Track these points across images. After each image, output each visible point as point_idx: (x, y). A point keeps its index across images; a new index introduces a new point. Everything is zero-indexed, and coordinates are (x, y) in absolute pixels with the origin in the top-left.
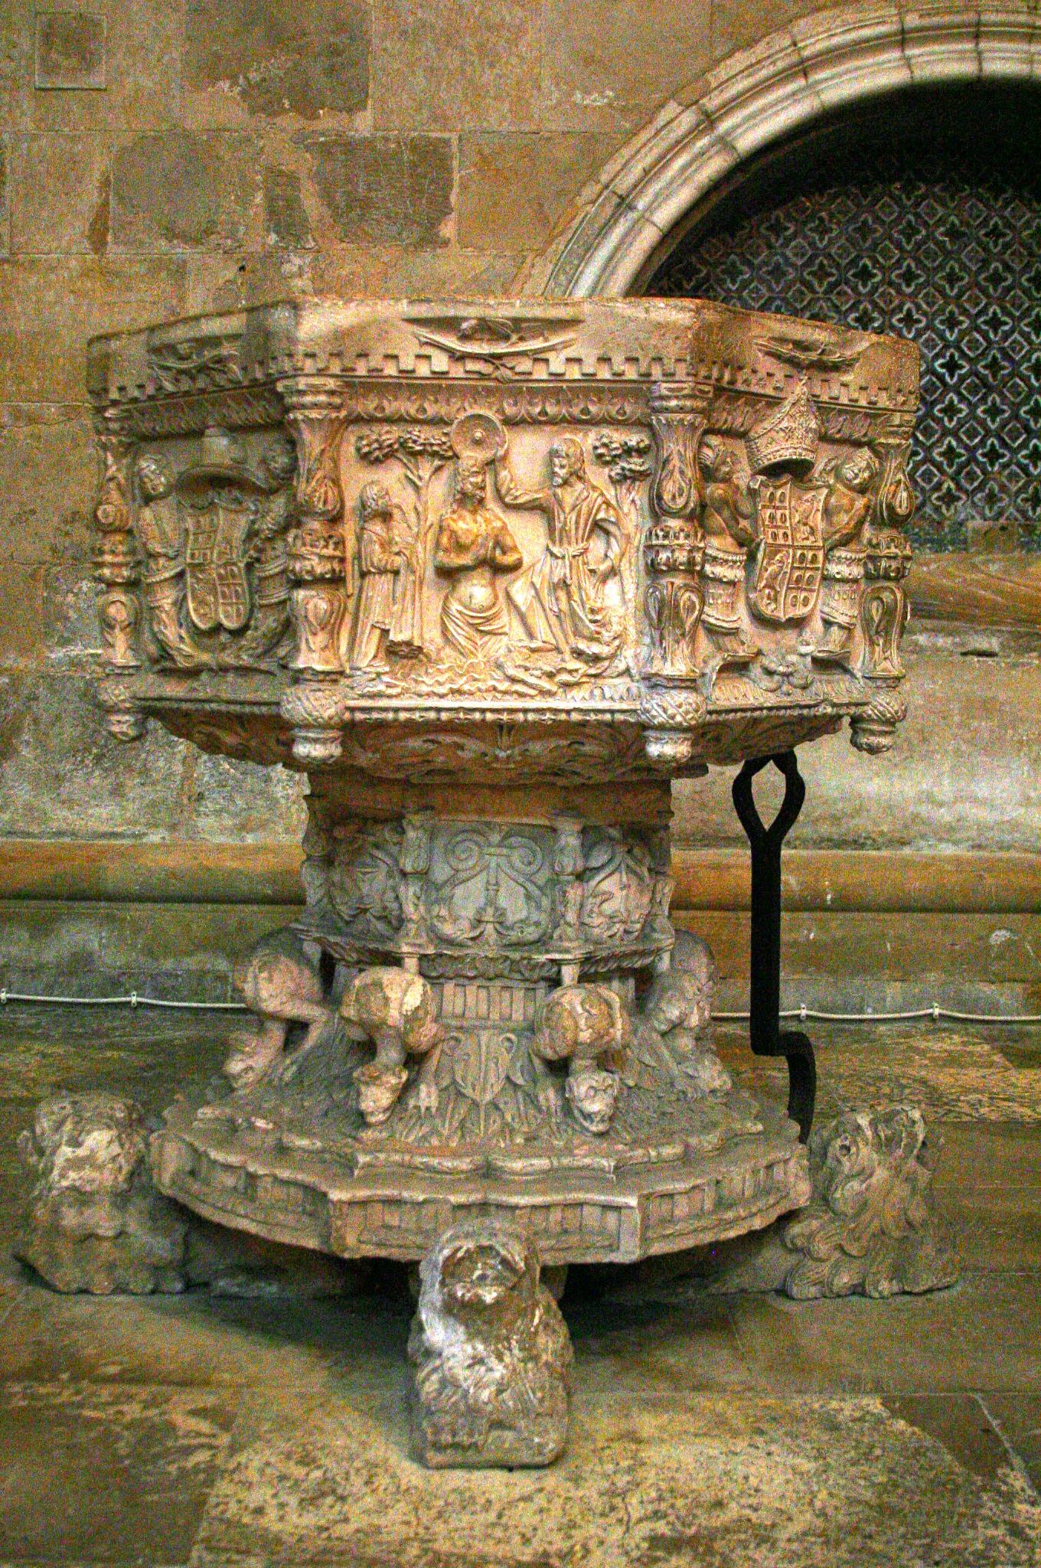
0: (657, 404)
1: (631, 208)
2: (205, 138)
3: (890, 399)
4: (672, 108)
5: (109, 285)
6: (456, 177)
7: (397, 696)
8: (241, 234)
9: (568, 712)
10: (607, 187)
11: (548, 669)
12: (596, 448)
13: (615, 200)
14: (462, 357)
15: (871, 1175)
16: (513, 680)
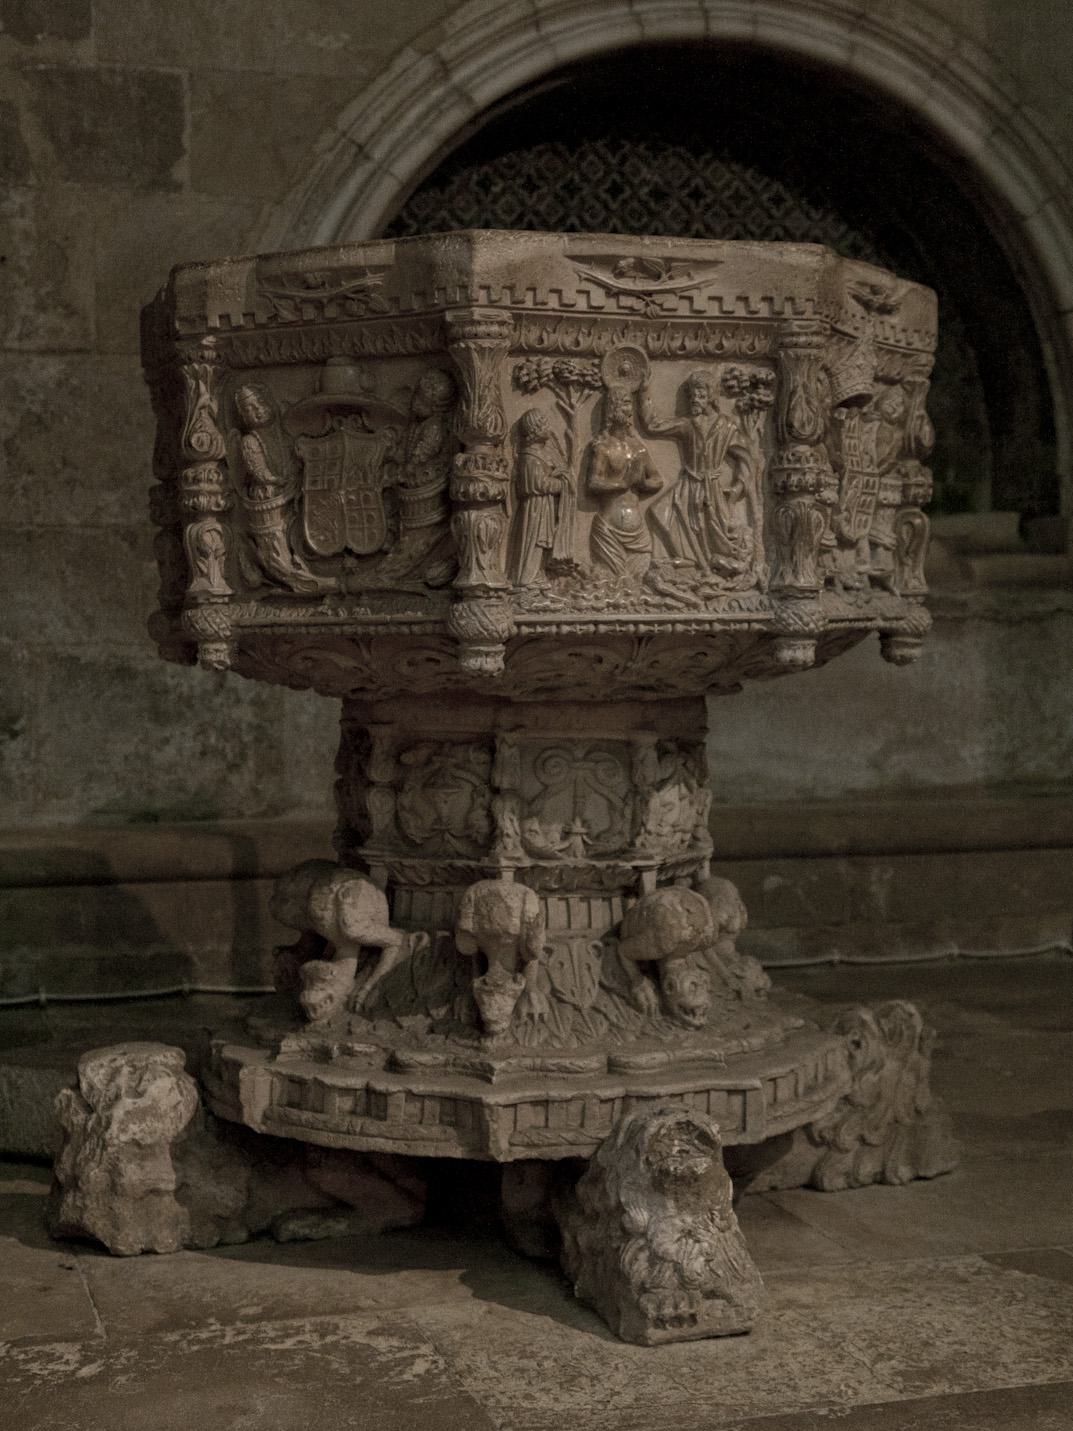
0: (787, 340)
1: (368, 158)
3: (921, 340)
4: (408, 57)
6: (188, 116)
9: (711, 622)
12: (726, 380)
13: (354, 149)
15: (882, 1066)
16: (663, 594)
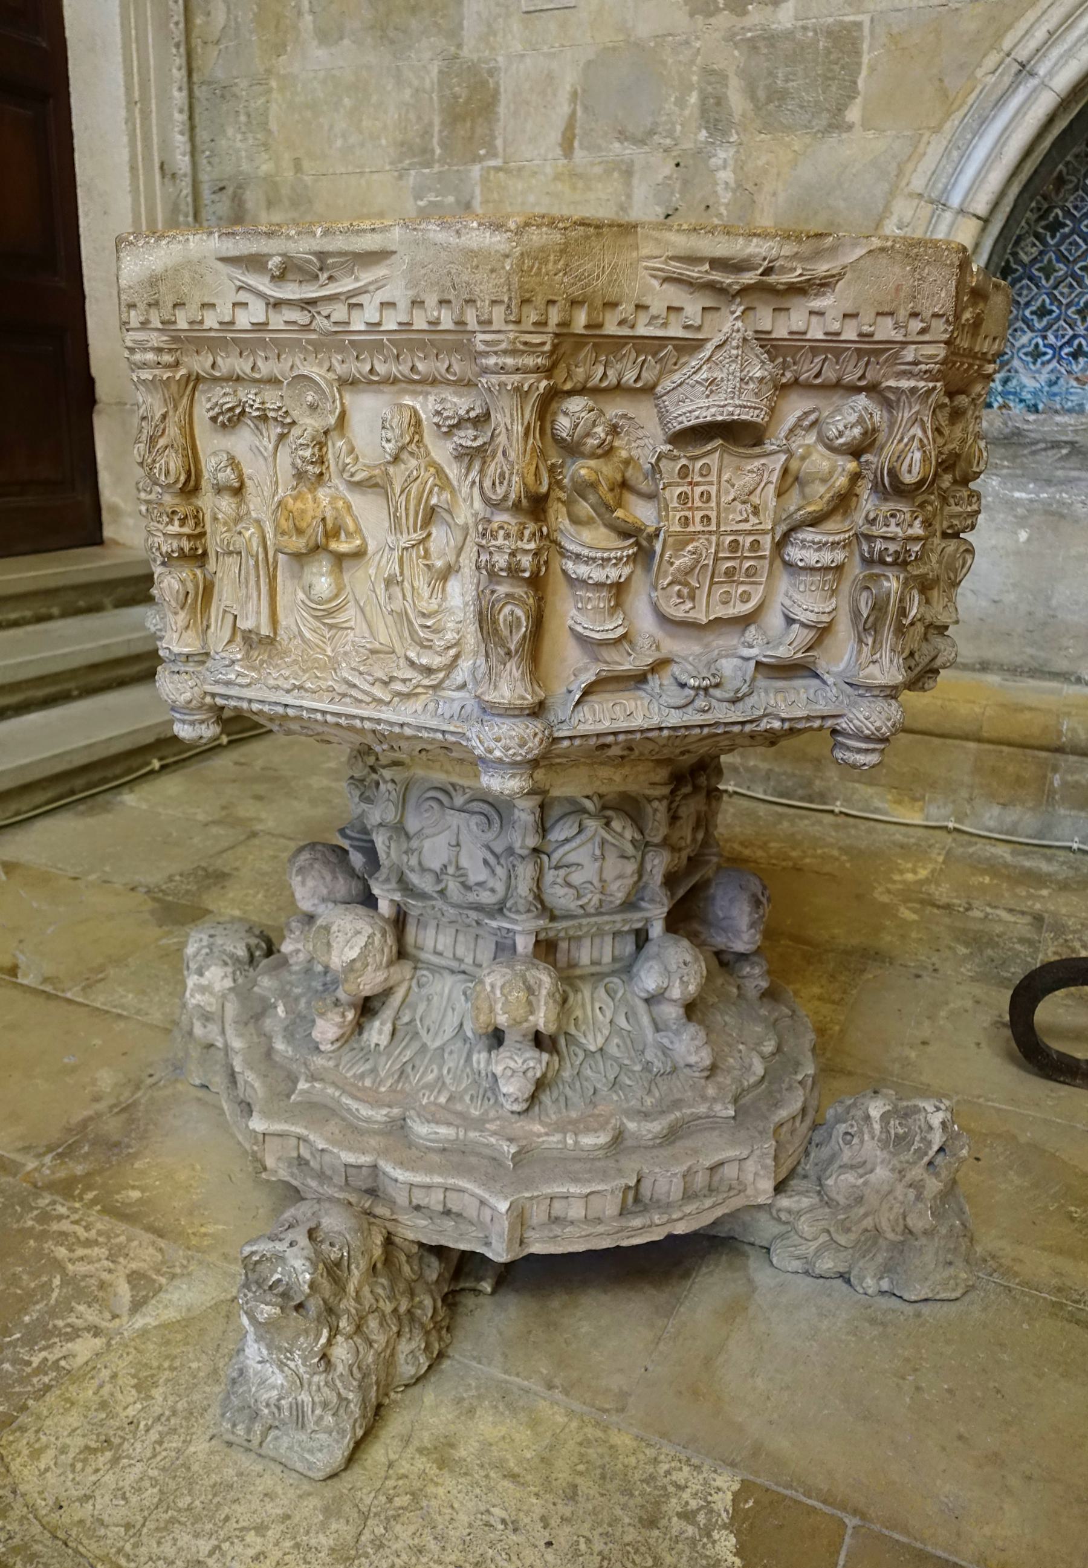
2: (652, 44)
5: (574, 188)
6: (865, 59)
7: (249, 685)
8: (678, 133)
10: (1008, 55)
11: (380, 674)
13: (1016, 67)
14: (277, 304)
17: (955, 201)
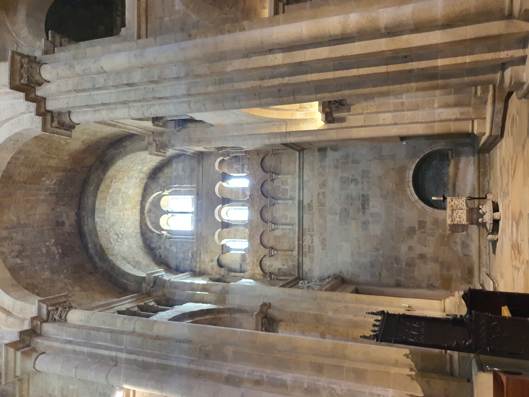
17: (432, 211)
